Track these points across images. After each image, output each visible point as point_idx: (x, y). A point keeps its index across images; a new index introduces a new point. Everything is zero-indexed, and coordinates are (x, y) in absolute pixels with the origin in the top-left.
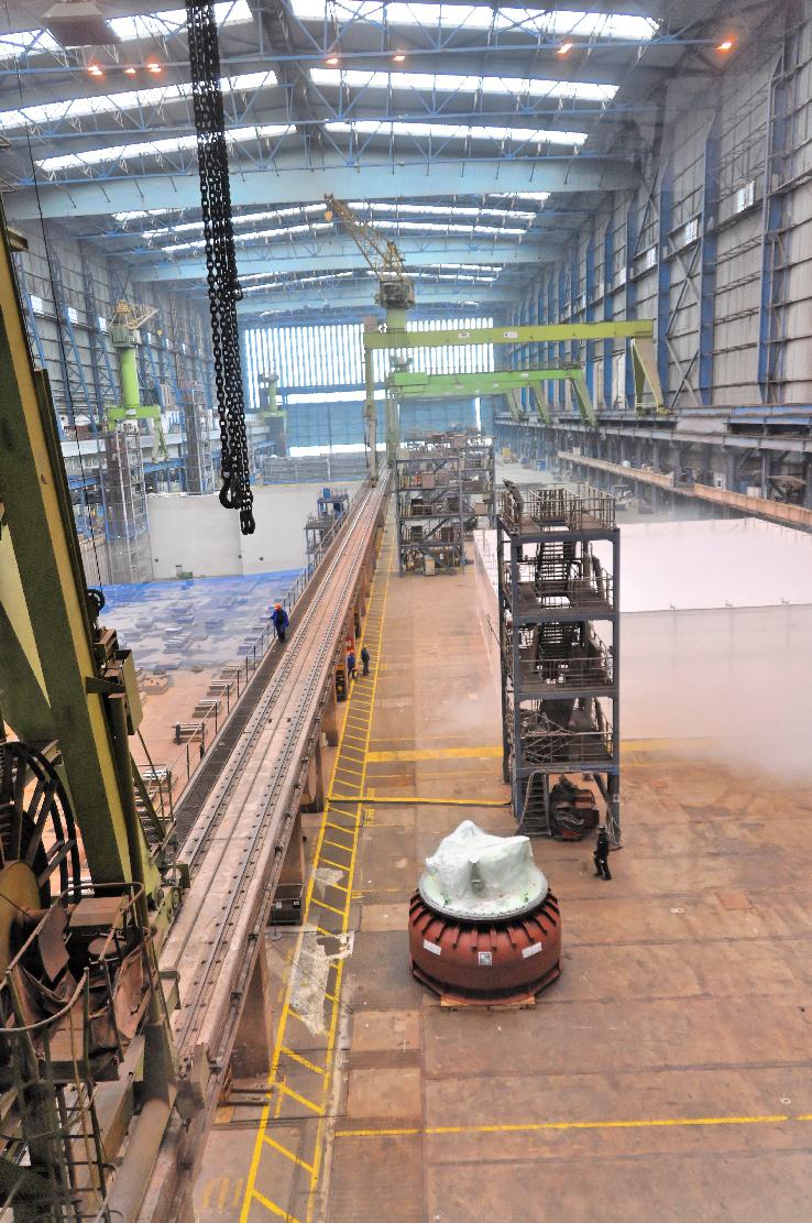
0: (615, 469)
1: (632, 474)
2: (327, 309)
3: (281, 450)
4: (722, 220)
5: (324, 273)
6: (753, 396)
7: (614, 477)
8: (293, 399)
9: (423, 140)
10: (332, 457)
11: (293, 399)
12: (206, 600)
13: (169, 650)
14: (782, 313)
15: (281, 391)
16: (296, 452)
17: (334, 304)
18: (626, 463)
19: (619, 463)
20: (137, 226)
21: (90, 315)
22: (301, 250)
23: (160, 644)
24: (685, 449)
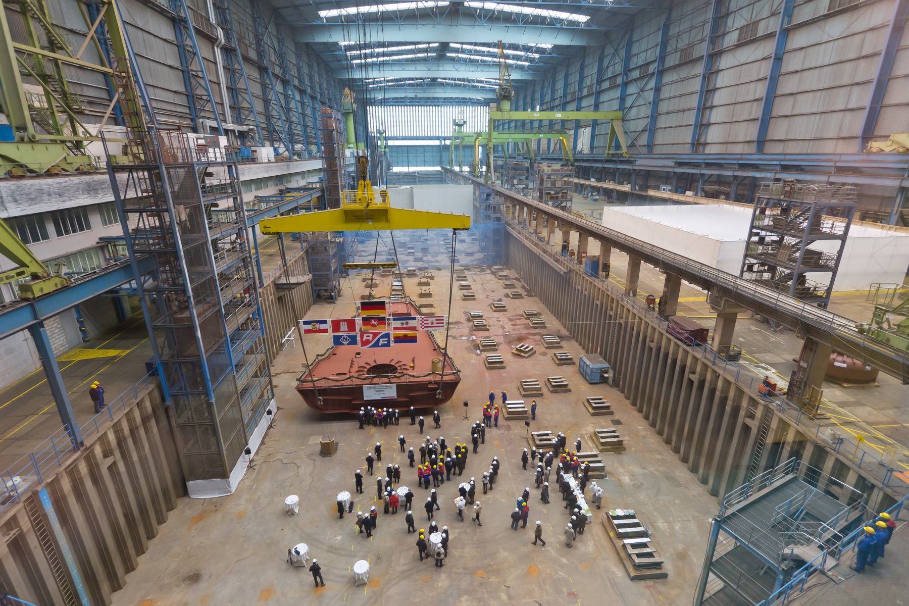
0: (587, 183)
1: (599, 184)
2: (416, 98)
3: (389, 168)
4: (666, 66)
5: (417, 79)
6: (753, 148)
7: (588, 186)
8: (390, 143)
9: (518, 14)
10: (419, 173)
11: (390, 143)
12: (408, 239)
13: (417, 260)
14: (708, 112)
15: (386, 139)
16: (396, 169)
17: (420, 95)
18: (593, 180)
19: (589, 179)
20: (350, 48)
21: (321, 95)
22: (421, 67)
23: (411, 258)
24: (638, 173)
